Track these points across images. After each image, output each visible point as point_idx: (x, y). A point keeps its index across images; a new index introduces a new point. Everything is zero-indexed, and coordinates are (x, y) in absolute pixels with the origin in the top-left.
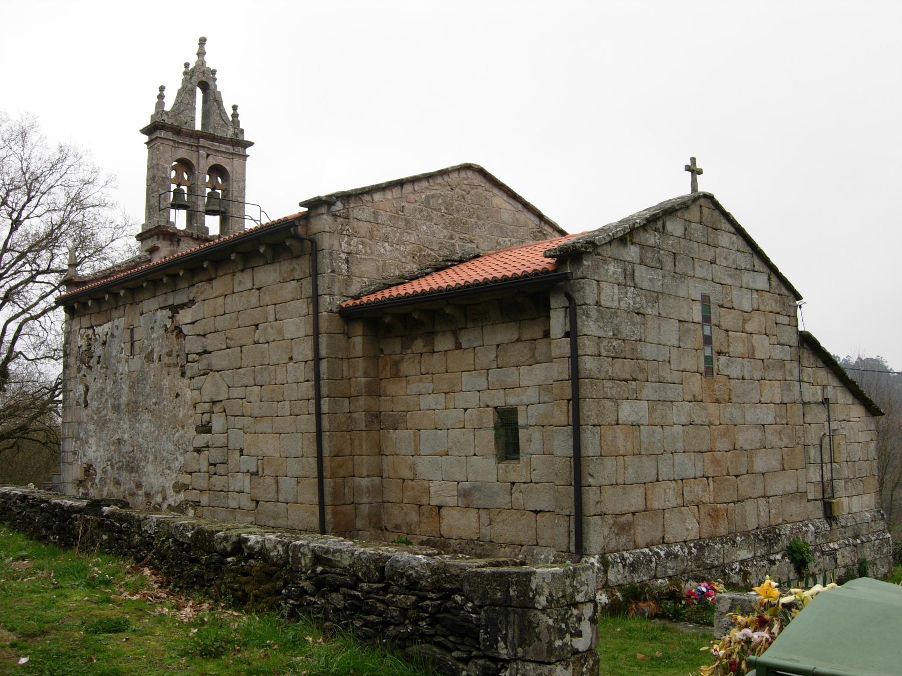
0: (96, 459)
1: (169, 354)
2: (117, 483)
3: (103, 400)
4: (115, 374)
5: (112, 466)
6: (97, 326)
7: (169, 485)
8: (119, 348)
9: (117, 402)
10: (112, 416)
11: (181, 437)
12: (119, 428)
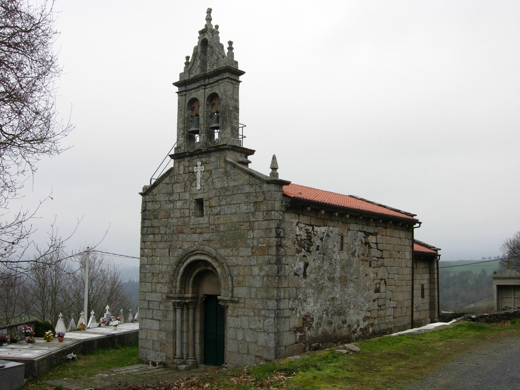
0: (314, 311)
1: (363, 255)
2: (330, 323)
3: (320, 274)
4: (331, 259)
5: (327, 314)
6: (316, 226)
7: (361, 318)
8: (333, 244)
9: (332, 276)
10: (327, 283)
11: (368, 295)
12: (333, 291)
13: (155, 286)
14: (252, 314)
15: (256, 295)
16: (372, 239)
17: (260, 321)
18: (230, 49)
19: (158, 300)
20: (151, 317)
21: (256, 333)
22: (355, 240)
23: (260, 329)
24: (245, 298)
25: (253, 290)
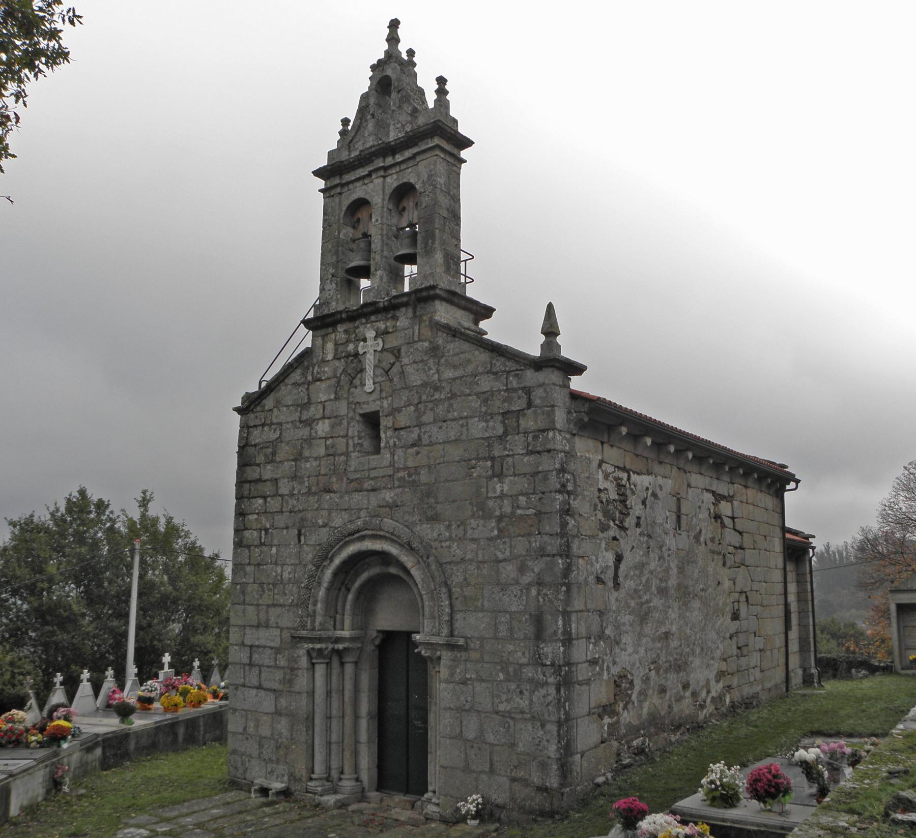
0: (634, 664)
1: (712, 540)
2: (663, 690)
3: (644, 580)
4: (661, 547)
5: (657, 670)
6: (634, 473)
7: (712, 676)
8: (662, 514)
9: (663, 585)
10: (657, 602)
11: (722, 624)
12: (667, 618)
13: (267, 612)
14: (501, 676)
15: (511, 630)
16: (725, 508)
17: (521, 692)
18: (442, 92)
19: (273, 644)
20: (256, 684)
21: (512, 723)
22: (700, 507)
23: (522, 712)
24: (482, 639)
25: (504, 618)
